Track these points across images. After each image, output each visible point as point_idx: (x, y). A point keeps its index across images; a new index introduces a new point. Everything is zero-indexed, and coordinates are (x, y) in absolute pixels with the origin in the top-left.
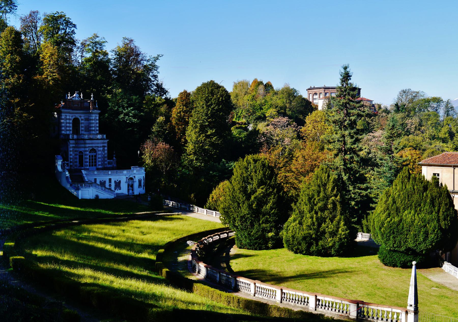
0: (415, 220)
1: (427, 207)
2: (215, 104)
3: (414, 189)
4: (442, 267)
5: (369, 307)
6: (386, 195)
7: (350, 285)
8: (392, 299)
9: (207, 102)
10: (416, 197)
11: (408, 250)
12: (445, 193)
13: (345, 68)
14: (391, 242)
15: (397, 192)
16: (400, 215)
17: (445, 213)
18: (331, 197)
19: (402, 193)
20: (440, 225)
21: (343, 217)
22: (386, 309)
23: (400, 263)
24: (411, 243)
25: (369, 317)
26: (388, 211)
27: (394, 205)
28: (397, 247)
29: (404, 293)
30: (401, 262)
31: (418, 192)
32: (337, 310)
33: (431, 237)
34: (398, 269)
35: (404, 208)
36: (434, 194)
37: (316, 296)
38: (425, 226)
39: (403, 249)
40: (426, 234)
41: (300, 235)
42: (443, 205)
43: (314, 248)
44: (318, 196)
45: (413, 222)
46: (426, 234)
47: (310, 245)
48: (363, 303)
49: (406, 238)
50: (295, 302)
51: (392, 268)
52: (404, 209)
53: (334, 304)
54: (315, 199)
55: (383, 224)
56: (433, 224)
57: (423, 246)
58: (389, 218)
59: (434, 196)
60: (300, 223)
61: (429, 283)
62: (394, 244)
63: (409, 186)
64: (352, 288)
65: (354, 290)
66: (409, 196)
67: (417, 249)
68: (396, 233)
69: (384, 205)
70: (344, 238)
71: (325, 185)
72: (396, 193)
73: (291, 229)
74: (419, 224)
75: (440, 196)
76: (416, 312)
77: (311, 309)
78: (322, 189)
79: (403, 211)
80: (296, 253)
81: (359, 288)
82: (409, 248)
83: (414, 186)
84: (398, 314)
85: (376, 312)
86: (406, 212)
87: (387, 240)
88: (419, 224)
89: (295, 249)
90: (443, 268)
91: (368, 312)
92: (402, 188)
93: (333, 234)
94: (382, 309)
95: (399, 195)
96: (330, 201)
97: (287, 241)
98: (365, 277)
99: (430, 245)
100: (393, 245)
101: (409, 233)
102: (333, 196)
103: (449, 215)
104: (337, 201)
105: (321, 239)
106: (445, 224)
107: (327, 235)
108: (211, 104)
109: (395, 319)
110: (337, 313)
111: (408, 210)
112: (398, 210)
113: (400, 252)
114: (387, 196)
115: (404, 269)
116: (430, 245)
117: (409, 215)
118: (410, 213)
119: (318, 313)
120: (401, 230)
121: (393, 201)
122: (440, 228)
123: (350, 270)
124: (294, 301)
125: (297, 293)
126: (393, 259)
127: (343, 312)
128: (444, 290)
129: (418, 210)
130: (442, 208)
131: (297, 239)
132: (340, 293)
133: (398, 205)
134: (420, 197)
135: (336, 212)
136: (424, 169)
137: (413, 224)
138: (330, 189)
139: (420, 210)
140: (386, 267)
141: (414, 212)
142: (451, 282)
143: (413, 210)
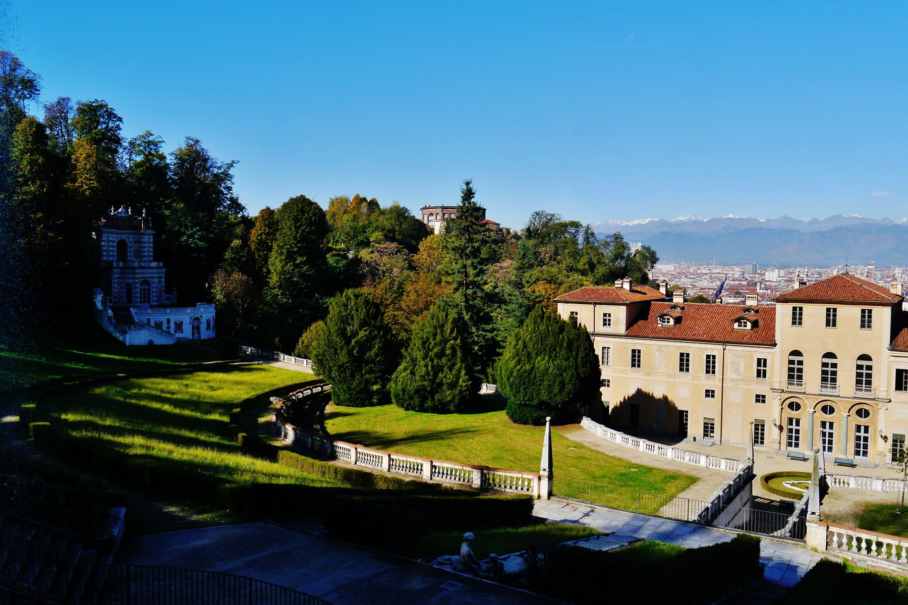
0: (549, 367)
1: (563, 352)
2: (305, 225)
3: (548, 331)
4: (580, 422)
5: (496, 473)
7: (472, 448)
8: (523, 463)
9: (296, 222)
10: (551, 340)
11: (541, 403)
13: (468, 184)
14: (521, 395)
15: (529, 334)
16: (532, 362)
17: (584, 359)
18: (450, 341)
20: (578, 374)
21: (464, 365)
22: (515, 475)
25: (495, 485)
28: (529, 400)
29: (536, 455)
31: (553, 334)
32: (457, 479)
33: (568, 388)
34: (530, 427)
35: (536, 353)
37: (432, 462)
38: (561, 375)
39: (535, 402)
40: (562, 384)
41: (411, 388)
43: (429, 403)
44: (434, 339)
45: (547, 370)
46: (562, 383)
47: (424, 400)
48: (488, 468)
49: (539, 389)
50: (406, 470)
51: (523, 426)
52: (537, 355)
53: (454, 471)
54: (430, 343)
55: (511, 373)
56: (570, 373)
57: (558, 399)
58: (519, 365)
59: (571, 339)
60: (413, 373)
61: (565, 442)
62: (524, 396)
63: (542, 328)
64: (475, 452)
65: (477, 453)
66: (543, 338)
70: (465, 391)
71: (442, 326)
73: (401, 380)
75: (578, 339)
76: (550, 477)
77: (426, 477)
78: (439, 331)
80: (407, 409)
81: (483, 451)
82: (543, 402)
83: (548, 327)
84: (529, 480)
85: (504, 479)
86: (539, 358)
87: (516, 392)
89: (406, 404)
90: (581, 424)
91: (494, 480)
92: (535, 330)
93: (452, 386)
94: (511, 475)
95: (531, 338)
96: (448, 345)
97: (397, 396)
98: (490, 437)
102: (452, 339)
103: (588, 361)
104: (457, 345)
105: (438, 392)
106: (584, 372)
107: (444, 388)
108: (302, 225)
109: (526, 486)
110: (457, 482)
111: (541, 355)
112: (529, 356)
113: (532, 406)
114: (516, 338)
115: (537, 427)
117: (543, 362)
118: (544, 358)
119: (435, 482)
121: (524, 345)
123: (472, 429)
124: (404, 469)
125: (409, 459)
126: (524, 415)
127: (464, 480)
128: (583, 450)
130: (580, 353)
131: (408, 392)
132: (461, 458)
134: (555, 340)
135: (456, 359)
136: (560, 306)
137: (547, 373)
138: (449, 331)
139: (555, 356)
140: (516, 425)
141: (548, 358)
142: (590, 440)
143: (547, 356)
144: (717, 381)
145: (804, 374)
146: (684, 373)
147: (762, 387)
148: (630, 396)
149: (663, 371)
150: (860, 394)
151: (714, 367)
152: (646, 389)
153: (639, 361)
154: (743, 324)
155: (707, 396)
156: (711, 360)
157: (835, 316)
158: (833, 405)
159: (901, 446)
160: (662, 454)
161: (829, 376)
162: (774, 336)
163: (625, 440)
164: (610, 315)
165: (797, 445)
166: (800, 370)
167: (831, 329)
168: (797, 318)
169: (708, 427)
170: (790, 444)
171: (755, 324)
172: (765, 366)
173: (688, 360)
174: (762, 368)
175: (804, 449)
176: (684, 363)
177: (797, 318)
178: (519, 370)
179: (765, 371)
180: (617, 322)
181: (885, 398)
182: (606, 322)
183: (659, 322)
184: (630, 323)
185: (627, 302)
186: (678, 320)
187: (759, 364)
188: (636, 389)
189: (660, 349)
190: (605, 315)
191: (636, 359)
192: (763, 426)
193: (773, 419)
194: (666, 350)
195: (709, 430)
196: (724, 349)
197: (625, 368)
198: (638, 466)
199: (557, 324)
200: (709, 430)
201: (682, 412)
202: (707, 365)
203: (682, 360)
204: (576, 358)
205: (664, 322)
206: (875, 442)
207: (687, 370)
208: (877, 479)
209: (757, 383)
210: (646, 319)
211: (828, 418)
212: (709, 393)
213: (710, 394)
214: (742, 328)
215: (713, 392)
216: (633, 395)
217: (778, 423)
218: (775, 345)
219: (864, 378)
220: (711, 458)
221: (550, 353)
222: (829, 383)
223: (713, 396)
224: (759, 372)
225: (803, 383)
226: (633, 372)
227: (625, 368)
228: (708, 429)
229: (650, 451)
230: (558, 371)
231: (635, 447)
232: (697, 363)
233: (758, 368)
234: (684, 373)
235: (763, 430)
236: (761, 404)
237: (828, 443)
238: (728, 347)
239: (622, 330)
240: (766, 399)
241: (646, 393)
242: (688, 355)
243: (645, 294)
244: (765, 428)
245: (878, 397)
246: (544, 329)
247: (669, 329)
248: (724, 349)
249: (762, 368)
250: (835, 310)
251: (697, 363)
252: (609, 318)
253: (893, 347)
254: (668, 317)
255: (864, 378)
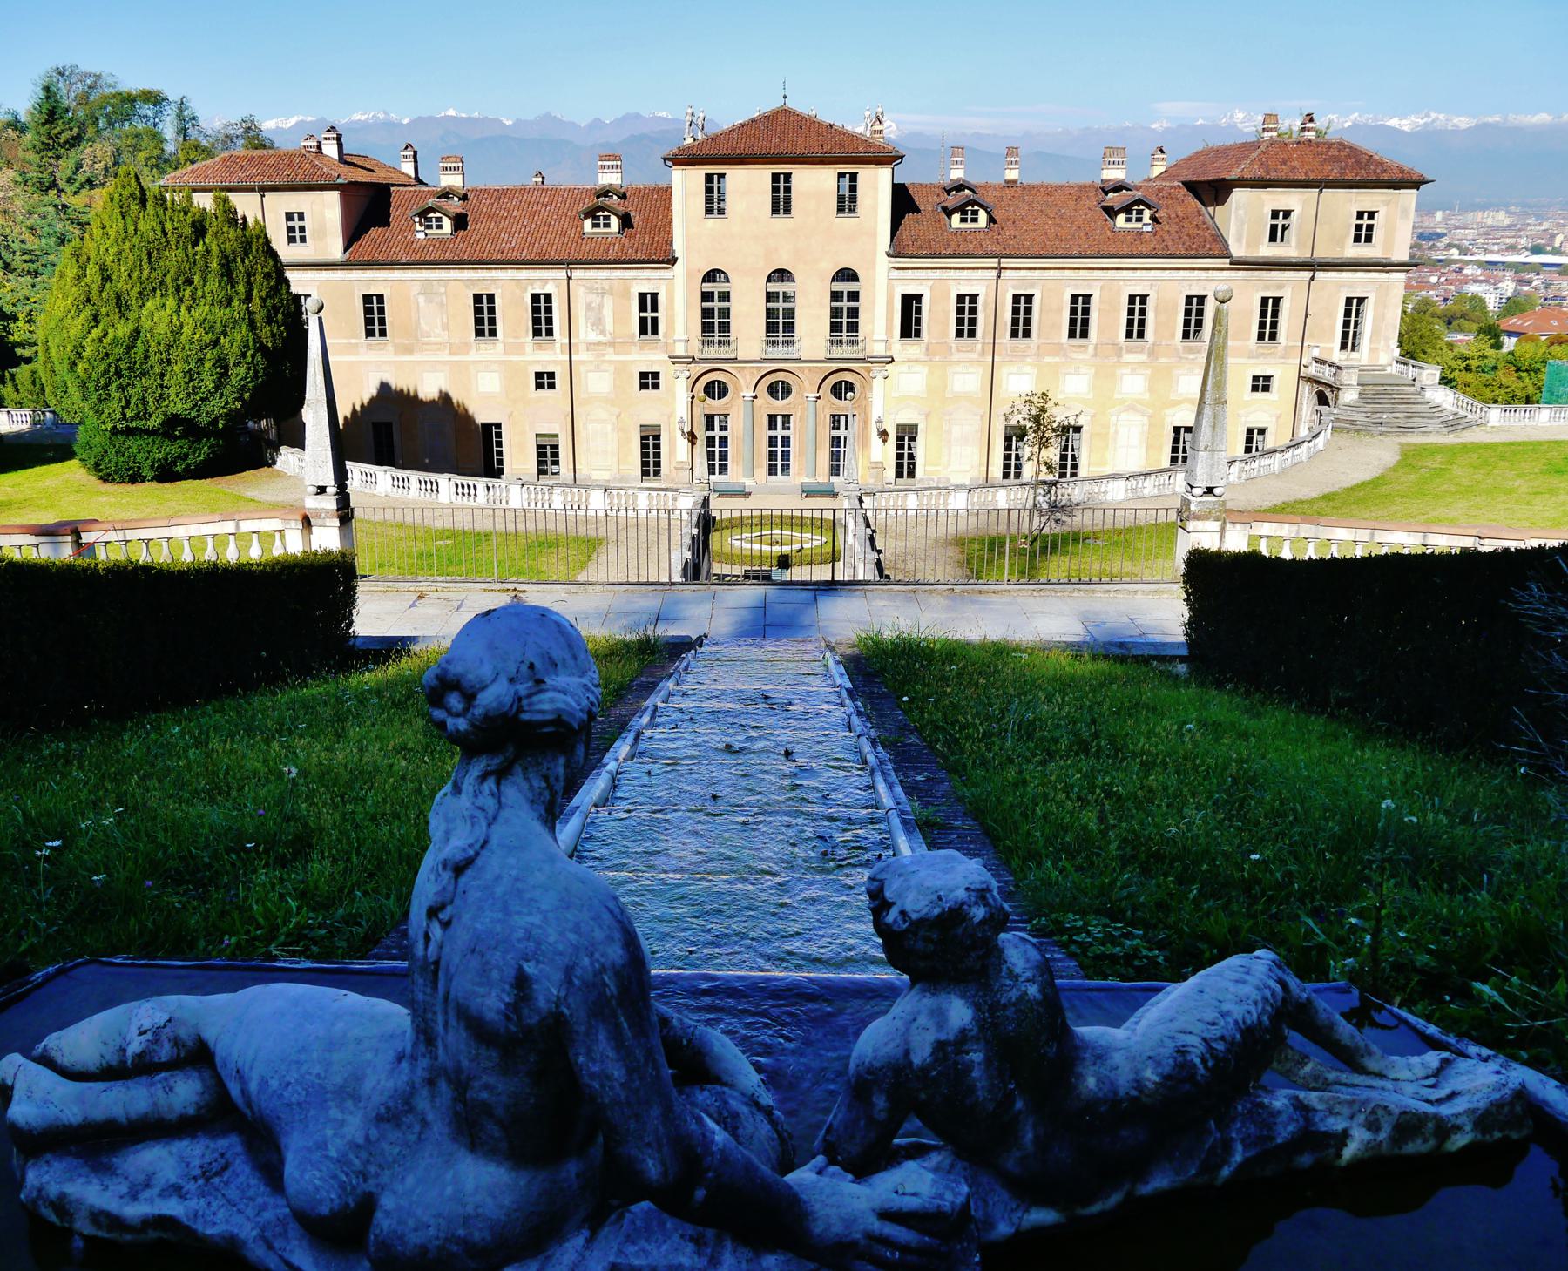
0: (182, 326)
1: (212, 285)
3: (165, 233)
4: (274, 463)
6: (74, 260)
10: (173, 258)
11: (172, 421)
12: (261, 241)
14: (114, 406)
17: (269, 303)
19: (127, 246)
20: (257, 340)
23: (152, 466)
24: (177, 400)
26: (89, 307)
27: (108, 285)
28: (137, 416)
30: (153, 462)
31: (178, 242)
34: (150, 489)
35: (140, 293)
36: (228, 245)
38: (216, 343)
39: (155, 421)
42: (259, 277)
46: (222, 365)
49: (162, 386)
51: (129, 487)
55: (78, 351)
56: (238, 337)
57: (215, 406)
59: (229, 251)
62: (124, 408)
63: (147, 225)
67: (199, 416)
68: (126, 373)
69: (74, 289)
72: (107, 250)
74: (197, 336)
75: (246, 253)
79: (140, 302)
82: (175, 416)
83: (162, 224)
88: (197, 336)
90: (278, 466)
95: (119, 253)
99: (237, 399)
100: (124, 415)
101: (169, 369)
106: (273, 335)
111: (154, 296)
112: (121, 303)
113: (147, 432)
115: (167, 485)
116: (237, 399)
118: (164, 306)
120: (142, 364)
122: (262, 348)
129: (187, 297)
133: (120, 285)
141: (175, 303)
144: (558, 351)
145: (734, 322)
146: (487, 339)
147: (651, 357)
148: (366, 403)
149: (438, 340)
150: (839, 352)
151: (549, 321)
152: (398, 382)
153: (382, 321)
154: (602, 222)
155: (539, 386)
156: (542, 305)
157: (788, 190)
158: (789, 379)
159: (910, 448)
160: (498, 502)
161: (780, 323)
162: (669, 242)
163: (401, 483)
164: (301, 216)
165: (723, 469)
166: (725, 313)
167: (781, 221)
168: (714, 203)
169: (545, 455)
170: (711, 470)
171: (626, 222)
172: (655, 309)
173: (492, 311)
174: (649, 315)
175: (736, 474)
176: (484, 317)
177: (714, 203)
178: (100, 341)
179: (655, 321)
180: (322, 233)
181: (883, 354)
182: (296, 234)
183: (418, 228)
184: (352, 236)
185: (339, 181)
186: (460, 222)
187: (642, 308)
188: (377, 384)
189: (427, 290)
190: (289, 216)
191: (374, 316)
192: (657, 437)
193: (678, 419)
194: (443, 290)
195: (549, 459)
196: (569, 278)
197: (353, 341)
198: (453, 534)
199: (186, 214)
200: (549, 459)
201: (487, 428)
202: (534, 319)
203: (478, 311)
204: (249, 298)
205: (430, 227)
206: (865, 443)
207: (493, 333)
208: (958, 488)
209: (642, 348)
210: (385, 223)
211: (779, 406)
212: (544, 380)
213: (546, 380)
214: (602, 230)
215: (551, 375)
216: (372, 400)
217: (686, 430)
218: (674, 261)
219: (845, 320)
220: (615, 492)
221: (178, 290)
222: (781, 334)
223: (552, 386)
224: (643, 321)
225: (731, 339)
226: (370, 347)
227: (353, 341)
228: (547, 456)
229: (465, 498)
230: (207, 333)
231: (428, 495)
232: (513, 315)
233: (643, 315)
234: (486, 341)
235: (657, 446)
236: (650, 392)
237: (778, 458)
238: (577, 274)
239: (336, 251)
240: (662, 380)
241: (402, 391)
242: (491, 298)
243: (372, 171)
244: (664, 441)
245: (868, 354)
246: (153, 229)
247: (442, 243)
248: (569, 278)
249: (649, 315)
250: (788, 177)
251: (513, 315)
252: (301, 223)
253: (896, 251)
254: (438, 215)
255: (845, 320)
